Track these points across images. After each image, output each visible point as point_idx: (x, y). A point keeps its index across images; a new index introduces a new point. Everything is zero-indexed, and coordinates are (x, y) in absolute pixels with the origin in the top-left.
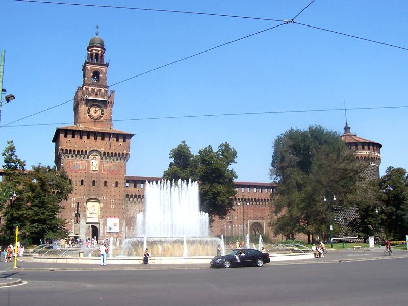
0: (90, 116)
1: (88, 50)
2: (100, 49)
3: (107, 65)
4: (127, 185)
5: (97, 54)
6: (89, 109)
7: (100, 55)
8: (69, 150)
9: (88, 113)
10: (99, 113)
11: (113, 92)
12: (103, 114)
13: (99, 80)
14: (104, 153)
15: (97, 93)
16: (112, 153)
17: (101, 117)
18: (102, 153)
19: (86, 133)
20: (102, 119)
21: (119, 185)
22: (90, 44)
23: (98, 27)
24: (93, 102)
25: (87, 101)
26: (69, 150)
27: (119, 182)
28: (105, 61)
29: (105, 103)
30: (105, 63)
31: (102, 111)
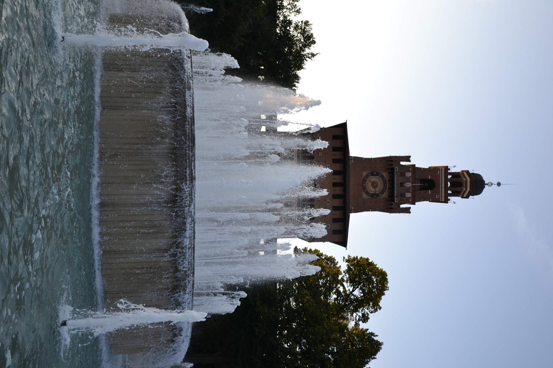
0: (367, 176)
1: (463, 171)
2: (468, 190)
3: (446, 201)
6: (377, 174)
7: (458, 189)
9: (372, 174)
11: (407, 211)
12: (372, 195)
15: (404, 186)
17: (367, 193)
20: (365, 195)
22: (473, 173)
23: (499, 184)
24: (389, 181)
25: (389, 171)
28: (452, 199)
29: (391, 197)
30: (449, 198)
31: (378, 195)
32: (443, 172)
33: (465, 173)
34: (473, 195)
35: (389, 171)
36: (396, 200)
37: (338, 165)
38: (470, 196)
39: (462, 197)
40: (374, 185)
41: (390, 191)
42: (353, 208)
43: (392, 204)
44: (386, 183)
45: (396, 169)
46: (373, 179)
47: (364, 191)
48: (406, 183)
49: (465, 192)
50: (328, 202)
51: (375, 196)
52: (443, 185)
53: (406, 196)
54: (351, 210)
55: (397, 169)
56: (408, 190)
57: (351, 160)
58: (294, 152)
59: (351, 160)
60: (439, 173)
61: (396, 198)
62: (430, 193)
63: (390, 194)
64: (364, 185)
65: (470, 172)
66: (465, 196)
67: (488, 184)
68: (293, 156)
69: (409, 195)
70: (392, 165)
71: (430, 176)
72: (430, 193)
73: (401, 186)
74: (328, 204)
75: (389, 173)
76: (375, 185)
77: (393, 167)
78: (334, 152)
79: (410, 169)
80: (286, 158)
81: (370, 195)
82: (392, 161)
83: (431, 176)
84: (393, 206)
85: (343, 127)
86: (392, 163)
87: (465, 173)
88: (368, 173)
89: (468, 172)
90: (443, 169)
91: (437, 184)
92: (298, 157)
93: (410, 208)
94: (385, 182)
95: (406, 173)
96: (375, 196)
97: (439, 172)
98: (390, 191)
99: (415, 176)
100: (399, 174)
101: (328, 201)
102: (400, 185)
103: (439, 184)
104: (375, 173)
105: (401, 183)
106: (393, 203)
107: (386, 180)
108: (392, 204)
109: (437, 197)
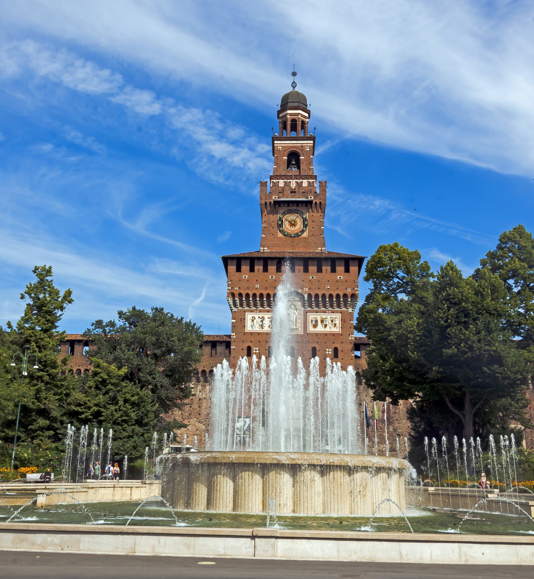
0: (282, 232)
1: (278, 117)
4: (358, 353)
5: (294, 121)
6: (281, 219)
8: (244, 295)
9: (281, 226)
10: (300, 225)
12: (305, 226)
13: (299, 168)
14: (310, 295)
16: (324, 296)
17: (303, 231)
18: (306, 296)
19: (275, 262)
20: (305, 235)
21: (340, 355)
22: (281, 106)
24: (288, 206)
25: (277, 206)
26: (244, 295)
27: (340, 349)
29: (308, 204)
31: (305, 220)
32: (279, 142)
33: (280, 115)
34: (307, 106)
35: (277, 206)
36: (311, 198)
37: (269, 267)
38: (308, 109)
39: (309, 117)
40: (293, 224)
41: (300, 205)
42: (320, 249)
43: (316, 203)
44: (291, 210)
45: (275, 198)
46: (286, 225)
47: (300, 235)
48: (292, 185)
49: (302, 116)
50: (313, 277)
51: (306, 223)
52: (295, 142)
53: (307, 185)
54: (321, 250)
55: (275, 198)
56: (299, 185)
57: (264, 250)
58: (255, 316)
59: (264, 250)
60: (281, 147)
61: (307, 198)
62: (303, 158)
63: (304, 205)
64: (293, 235)
65: (280, 109)
66: (307, 115)
67: (294, 87)
68: (259, 318)
69: (305, 183)
70: (270, 203)
71: (284, 158)
72: (303, 158)
73: (295, 192)
74: (314, 278)
75: (279, 206)
76: (293, 222)
77: (272, 202)
78: (255, 271)
79: (274, 181)
80: (261, 325)
81: (305, 229)
82: (266, 203)
83: (283, 156)
84: (318, 202)
85: (226, 261)
86: (268, 203)
87: (280, 115)
88: (280, 231)
89: (279, 112)
90: (275, 142)
91: (294, 149)
92: (260, 312)
93: (319, 182)
94: (290, 211)
95: (280, 186)
96: (306, 223)
97: (279, 147)
98: (300, 205)
99: (283, 176)
100: (281, 195)
101: (311, 277)
102: (293, 194)
103: (293, 147)
104: (280, 223)
105: (291, 192)
106: (314, 202)
107: (288, 210)
108: (316, 203)
109: (308, 149)
